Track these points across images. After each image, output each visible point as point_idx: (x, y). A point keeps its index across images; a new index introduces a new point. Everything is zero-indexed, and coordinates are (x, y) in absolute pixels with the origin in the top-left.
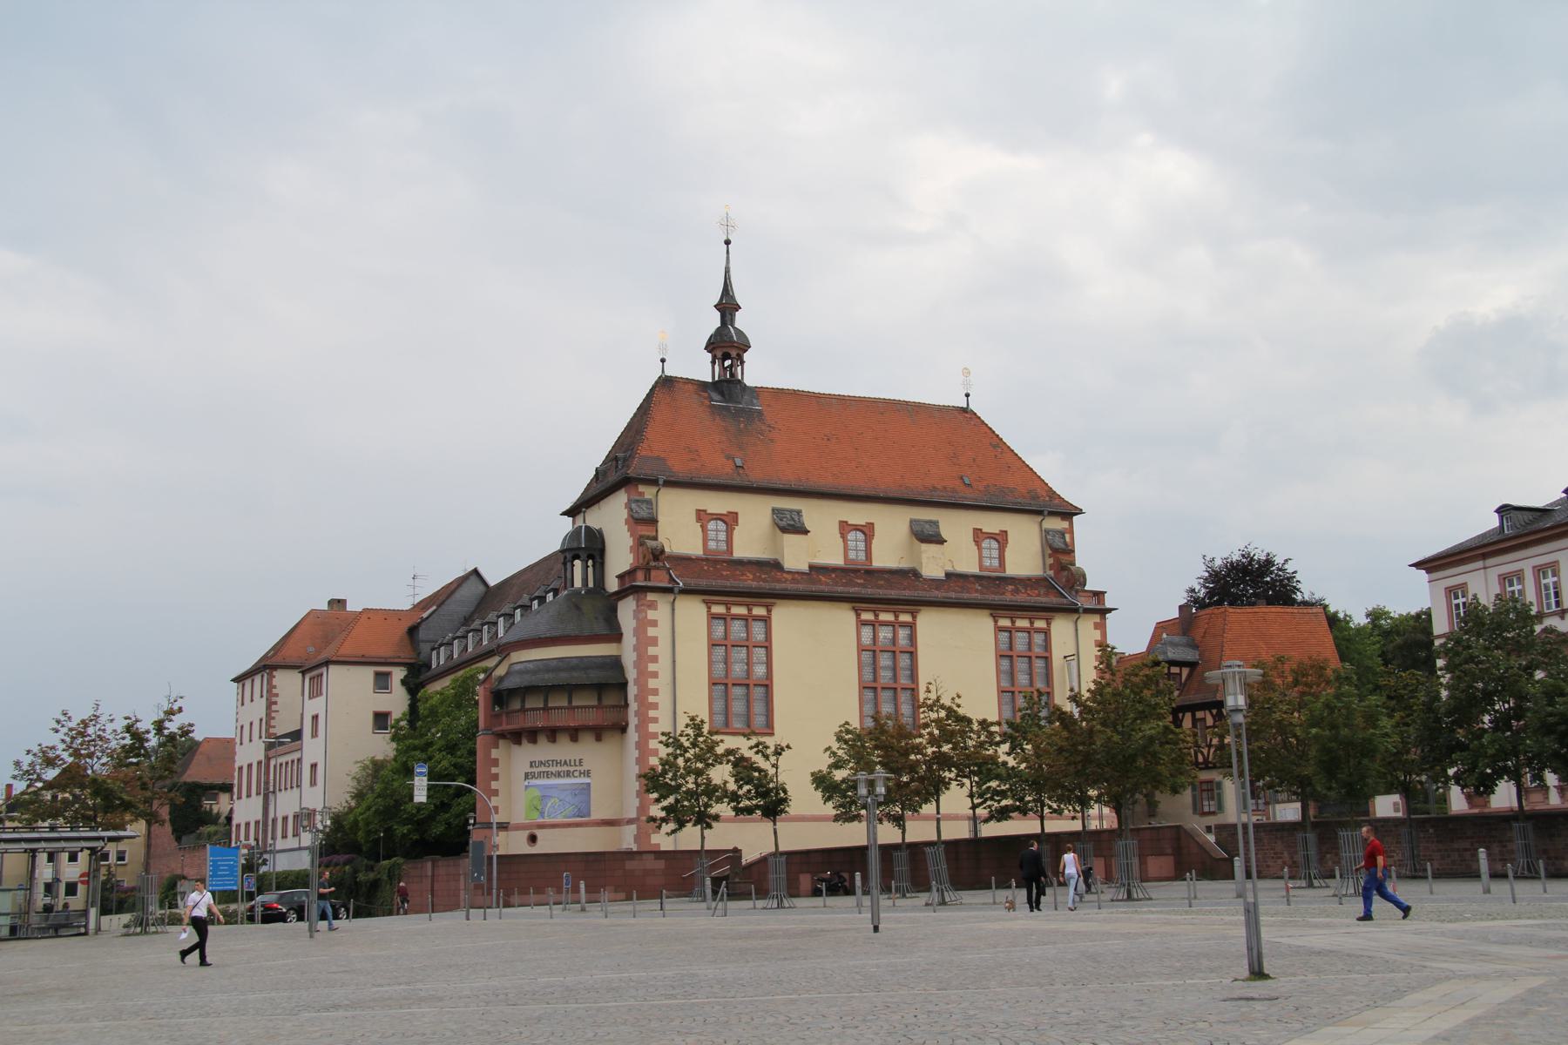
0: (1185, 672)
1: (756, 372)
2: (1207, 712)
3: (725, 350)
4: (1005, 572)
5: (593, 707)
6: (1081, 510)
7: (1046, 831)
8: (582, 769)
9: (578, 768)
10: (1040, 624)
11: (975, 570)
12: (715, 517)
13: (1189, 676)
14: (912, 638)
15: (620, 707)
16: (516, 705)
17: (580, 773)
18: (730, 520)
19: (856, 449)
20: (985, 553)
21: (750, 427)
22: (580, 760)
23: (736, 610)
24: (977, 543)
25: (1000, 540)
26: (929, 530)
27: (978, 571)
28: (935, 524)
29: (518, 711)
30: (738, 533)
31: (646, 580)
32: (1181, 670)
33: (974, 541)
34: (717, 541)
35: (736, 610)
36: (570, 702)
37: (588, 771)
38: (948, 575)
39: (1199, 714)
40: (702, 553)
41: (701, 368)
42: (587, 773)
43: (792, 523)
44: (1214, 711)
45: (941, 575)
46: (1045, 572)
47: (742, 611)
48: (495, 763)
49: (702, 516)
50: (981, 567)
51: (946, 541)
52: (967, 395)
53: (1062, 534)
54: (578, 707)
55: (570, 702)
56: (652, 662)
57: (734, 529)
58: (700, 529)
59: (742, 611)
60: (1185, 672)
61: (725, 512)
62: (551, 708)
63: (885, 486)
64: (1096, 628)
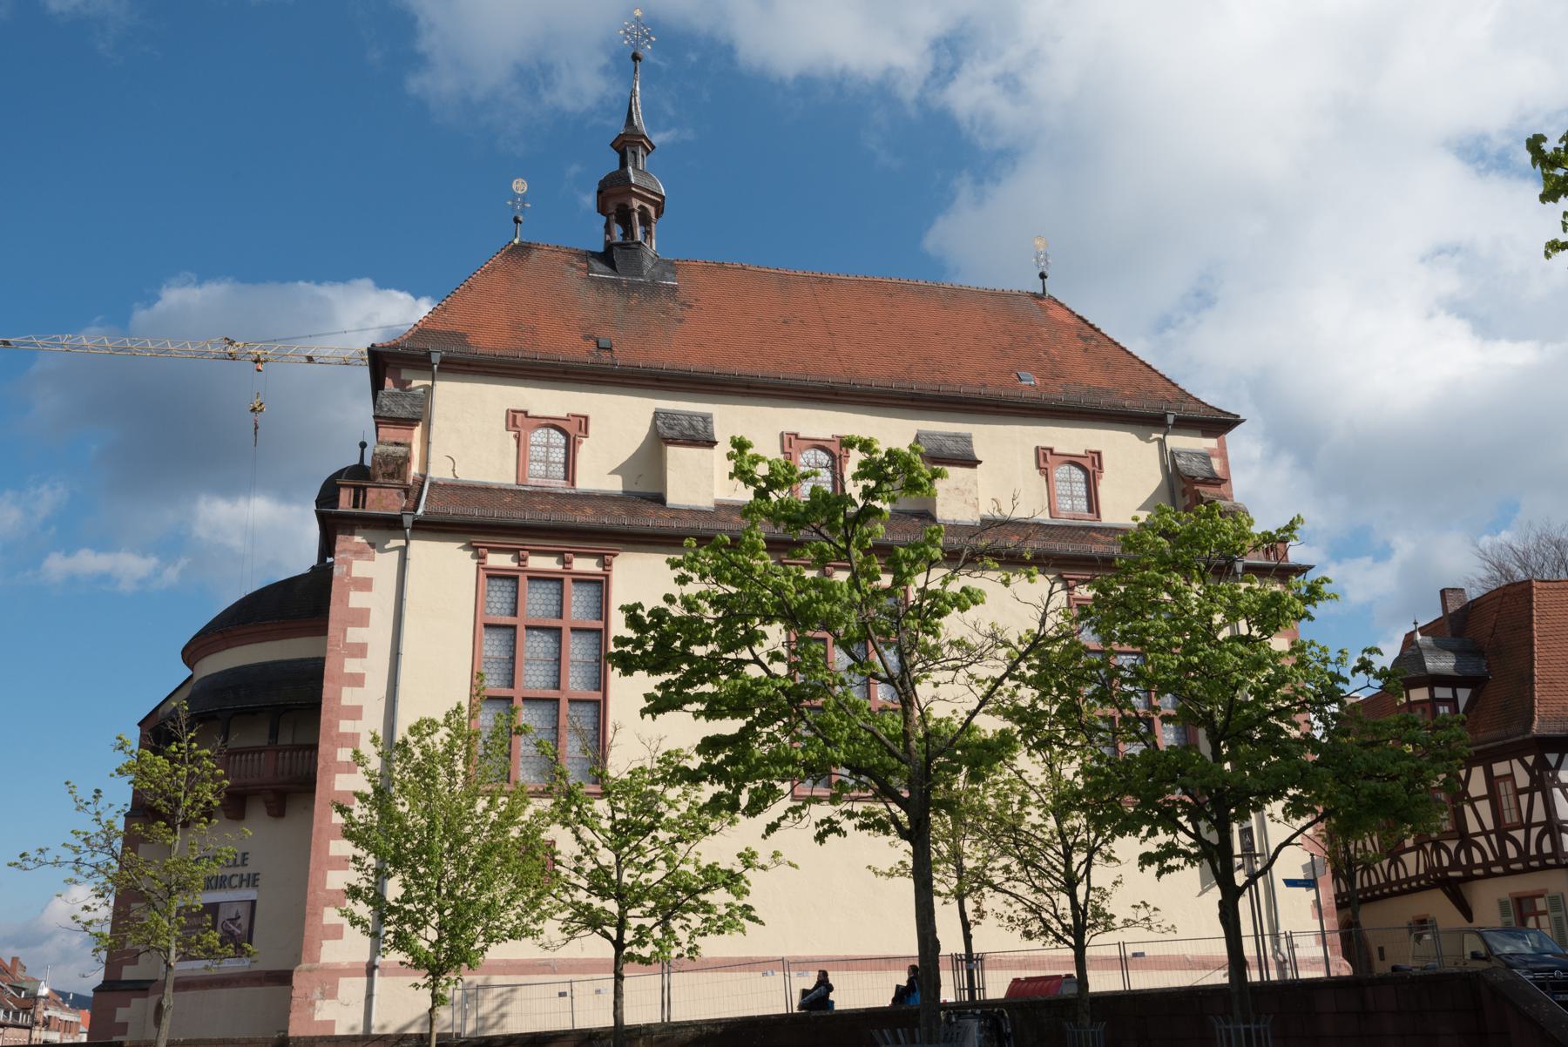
0: (1464, 695)
2: (1515, 762)
3: (620, 201)
5: (258, 750)
6: (1238, 416)
7: (672, 1020)
8: (244, 871)
9: (239, 871)
11: (1044, 517)
12: (544, 422)
13: (1471, 703)
17: (241, 881)
18: (572, 431)
20: (1061, 488)
22: (244, 854)
23: (537, 563)
24: (1044, 471)
25: (1090, 468)
26: (952, 448)
27: (1048, 518)
28: (967, 440)
30: (586, 452)
31: (354, 507)
32: (1455, 694)
33: (1039, 467)
34: (547, 463)
35: (537, 563)
37: (255, 875)
38: (984, 521)
39: (1500, 768)
40: (512, 481)
42: (252, 881)
44: (1530, 760)
47: (549, 564)
51: (980, 462)
53: (1206, 457)
56: (353, 656)
57: (580, 442)
58: (514, 442)
59: (549, 564)
60: (1464, 695)
61: (564, 415)
63: (876, 374)
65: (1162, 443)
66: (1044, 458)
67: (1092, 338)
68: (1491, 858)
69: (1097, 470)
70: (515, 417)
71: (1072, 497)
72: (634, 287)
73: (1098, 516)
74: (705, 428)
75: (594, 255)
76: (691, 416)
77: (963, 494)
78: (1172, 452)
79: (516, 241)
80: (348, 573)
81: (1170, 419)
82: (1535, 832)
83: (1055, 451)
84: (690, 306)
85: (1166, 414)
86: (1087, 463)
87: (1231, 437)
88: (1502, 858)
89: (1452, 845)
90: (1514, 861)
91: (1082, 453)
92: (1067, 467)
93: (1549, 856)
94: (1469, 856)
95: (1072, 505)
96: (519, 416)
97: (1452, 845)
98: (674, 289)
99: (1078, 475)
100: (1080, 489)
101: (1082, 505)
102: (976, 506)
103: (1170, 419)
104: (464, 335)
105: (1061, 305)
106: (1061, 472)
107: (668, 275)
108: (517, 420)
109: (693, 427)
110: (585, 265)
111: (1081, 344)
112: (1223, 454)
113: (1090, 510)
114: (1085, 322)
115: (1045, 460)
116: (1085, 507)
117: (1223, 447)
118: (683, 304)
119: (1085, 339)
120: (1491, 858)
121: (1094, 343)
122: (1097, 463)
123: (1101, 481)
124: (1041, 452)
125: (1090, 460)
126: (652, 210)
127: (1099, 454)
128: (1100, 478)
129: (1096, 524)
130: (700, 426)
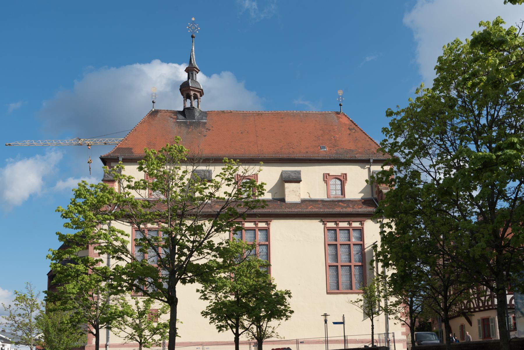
10: (356, 225)
14: (268, 238)
19: (257, 136)
20: (332, 187)
21: (194, 130)
27: (326, 198)
28: (299, 172)
33: (324, 181)
38: (304, 201)
45: (297, 200)
46: (373, 196)
50: (328, 196)
63: (268, 152)
65: (369, 169)
66: (326, 177)
67: (354, 129)
68: (475, 306)
69: (345, 180)
71: (336, 190)
72: (191, 124)
73: (344, 196)
74: (209, 175)
75: (179, 112)
77: (295, 192)
78: (373, 172)
79: (153, 110)
81: (371, 161)
82: (487, 298)
83: (330, 174)
84: (209, 130)
85: (370, 159)
86: (342, 178)
88: (478, 306)
89: (465, 302)
90: (481, 307)
92: (334, 180)
93: (490, 305)
94: (470, 305)
95: (335, 193)
97: (465, 302)
98: (205, 123)
99: (338, 182)
100: (339, 187)
101: (339, 192)
102: (299, 196)
103: (371, 161)
104: (131, 149)
106: (332, 182)
107: (204, 118)
110: (175, 117)
111: (349, 132)
113: (342, 194)
114: (353, 122)
115: (326, 178)
116: (340, 193)
118: (207, 129)
119: (350, 129)
120: (475, 306)
121: (354, 131)
122: (345, 178)
123: (346, 184)
124: (325, 175)
125: (343, 177)
126: (198, 95)
127: (346, 174)
128: (346, 183)
129: (344, 199)
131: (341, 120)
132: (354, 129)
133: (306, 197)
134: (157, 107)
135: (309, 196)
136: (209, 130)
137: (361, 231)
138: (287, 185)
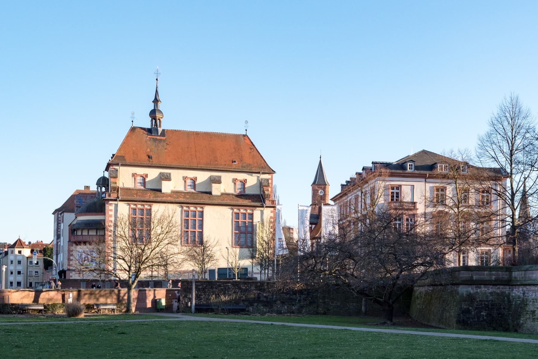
1: (166, 124)
4: (245, 193)
6: (275, 172)
15: (103, 235)
16: (79, 233)
21: (159, 144)
28: (220, 177)
29: (80, 235)
36: (88, 233)
38: (222, 194)
41: (147, 123)
43: (167, 177)
45: (219, 194)
48: (72, 251)
49: (134, 175)
52: (246, 130)
53: (268, 180)
54: (90, 235)
55: (88, 233)
58: (134, 179)
62: (84, 235)
64: (271, 212)
67: (253, 149)
70: (134, 175)
76: (167, 173)
78: (261, 179)
80: (109, 208)
87: (274, 175)
91: (242, 179)
96: (135, 174)
102: (220, 191)
104: (124, 157)
105: (249, 138)
108: (134, 175)
109: (167, 176)
111: (250, 151)
112: (272, 179)
117: (272, 177)
119: (251, 149)
129: (244, 194)
130: (169, 176)
131: (246, 141)
132: (253, 149)
133: (223, 191)
134: (135, 125)
135: (225, 191)
136: (168, 144)
137: (252, 215)
138: (213, 185)
